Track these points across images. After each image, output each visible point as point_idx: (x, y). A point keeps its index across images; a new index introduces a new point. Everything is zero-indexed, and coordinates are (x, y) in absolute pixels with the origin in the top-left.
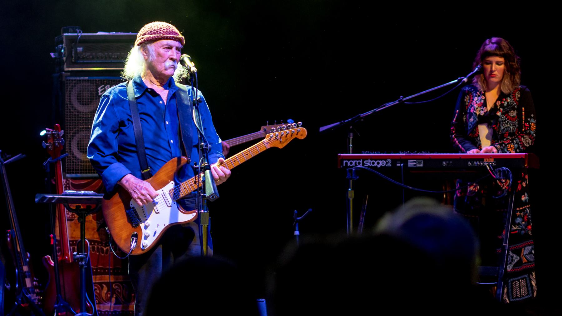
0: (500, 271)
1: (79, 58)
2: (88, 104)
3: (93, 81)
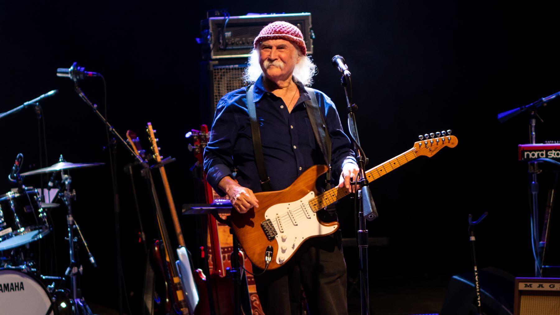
1: (227, 45)
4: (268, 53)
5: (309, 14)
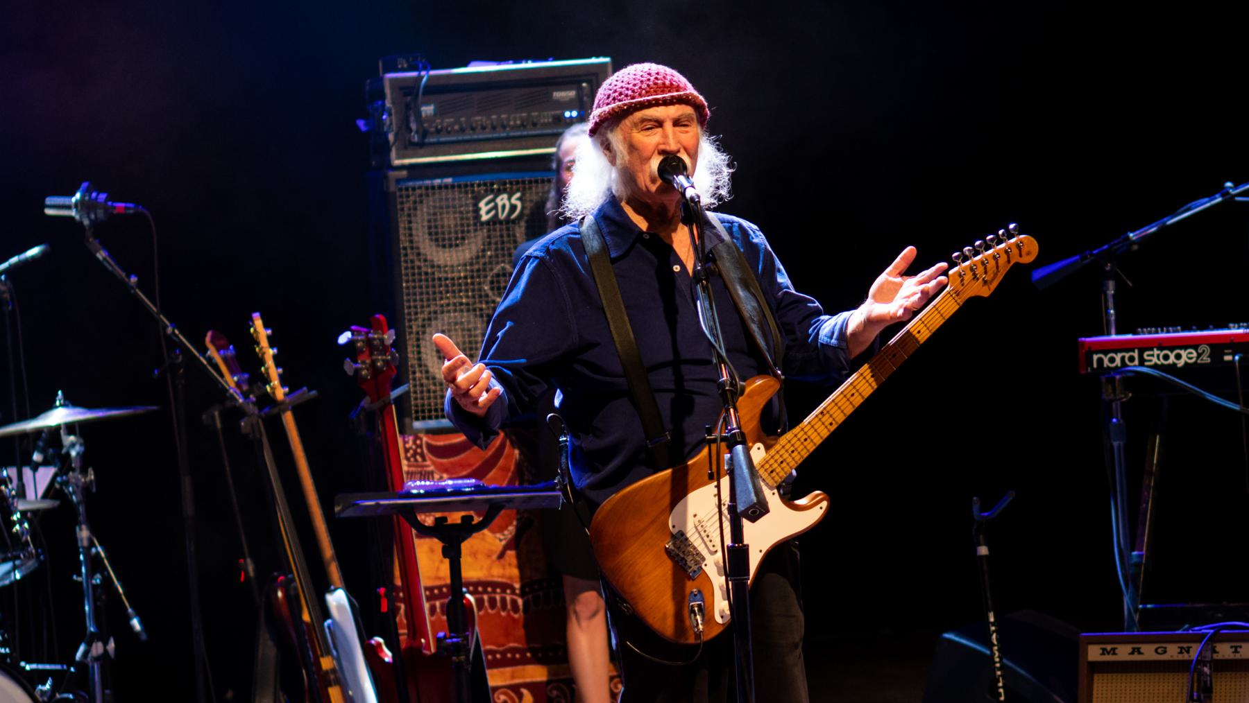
2: (457, 245)
3: (466, 186)
5: (607, 60)
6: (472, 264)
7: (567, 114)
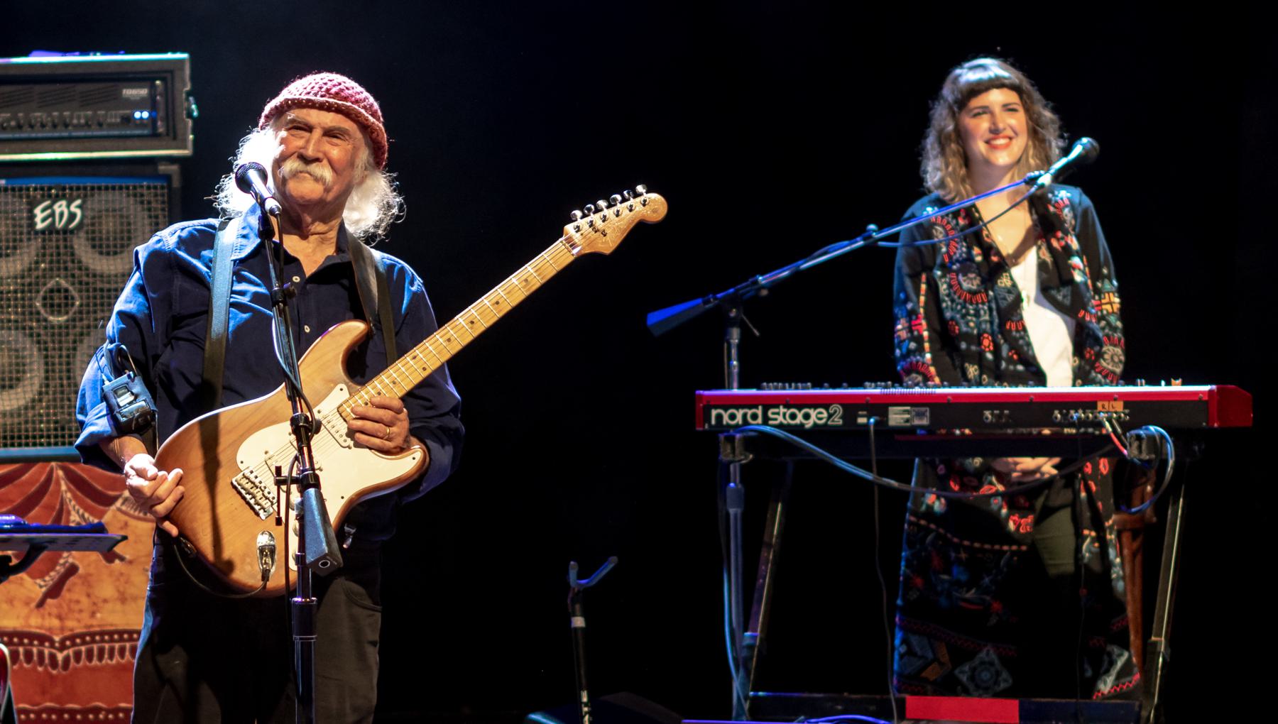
0: (1144, 714)
3: (21, 189)
4: (300, 143)
5: (185, 56)
6: (23, 277)
7: (137, 115)
